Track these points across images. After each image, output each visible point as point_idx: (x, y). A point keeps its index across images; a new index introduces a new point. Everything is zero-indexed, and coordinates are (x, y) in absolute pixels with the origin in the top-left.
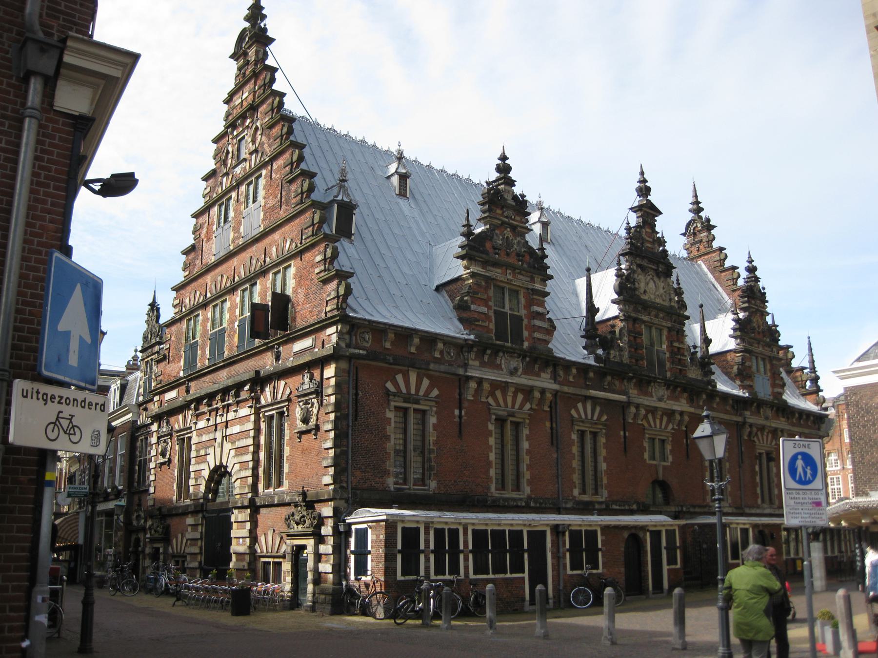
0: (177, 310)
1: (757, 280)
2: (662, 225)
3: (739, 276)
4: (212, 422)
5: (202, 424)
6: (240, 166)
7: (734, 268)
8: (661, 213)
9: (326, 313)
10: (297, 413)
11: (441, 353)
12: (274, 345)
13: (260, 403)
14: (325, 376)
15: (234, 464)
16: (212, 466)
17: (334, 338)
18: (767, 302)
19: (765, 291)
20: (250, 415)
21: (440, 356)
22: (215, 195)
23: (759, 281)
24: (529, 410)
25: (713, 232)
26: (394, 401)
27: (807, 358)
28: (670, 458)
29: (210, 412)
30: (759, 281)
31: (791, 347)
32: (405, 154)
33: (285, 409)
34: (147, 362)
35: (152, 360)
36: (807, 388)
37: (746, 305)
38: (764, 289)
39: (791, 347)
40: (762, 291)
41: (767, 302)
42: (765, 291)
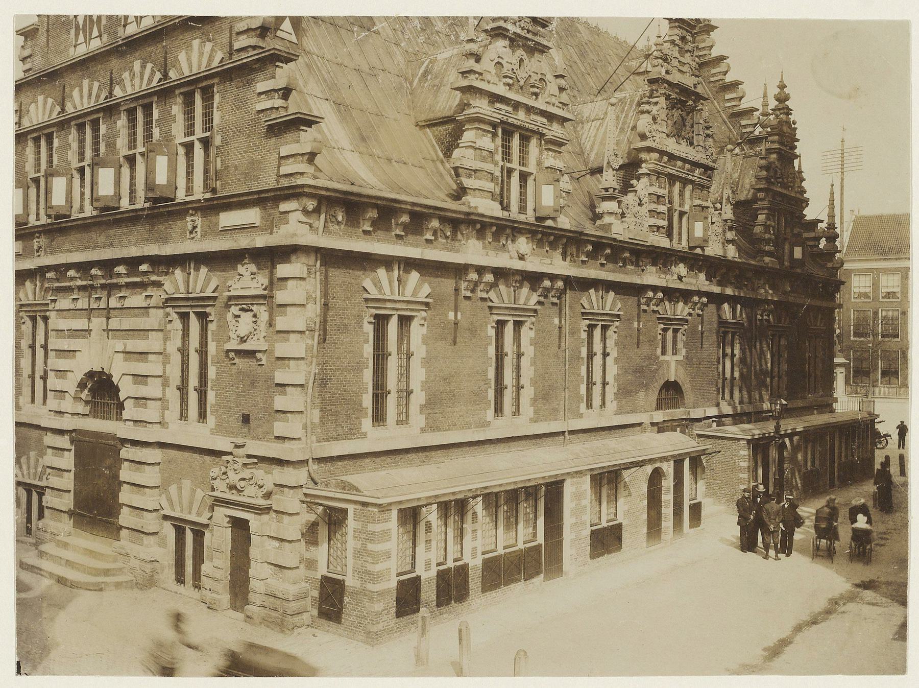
1: (788, 111)
5: (64, 303)
11: (435, 233)
12: (188, 209)
18: (798, 140)
19: (796, 126)
21: (433, 238)
23: (791, 114)
26: (374, 308)
27: (827, 211)
28: (684, 352)
30: (791, 114)
36: (821, 246)
37: (776, 146)
38: (794, 123)
40: (793, 126)
41: (798, 140)
42: (796, 126)
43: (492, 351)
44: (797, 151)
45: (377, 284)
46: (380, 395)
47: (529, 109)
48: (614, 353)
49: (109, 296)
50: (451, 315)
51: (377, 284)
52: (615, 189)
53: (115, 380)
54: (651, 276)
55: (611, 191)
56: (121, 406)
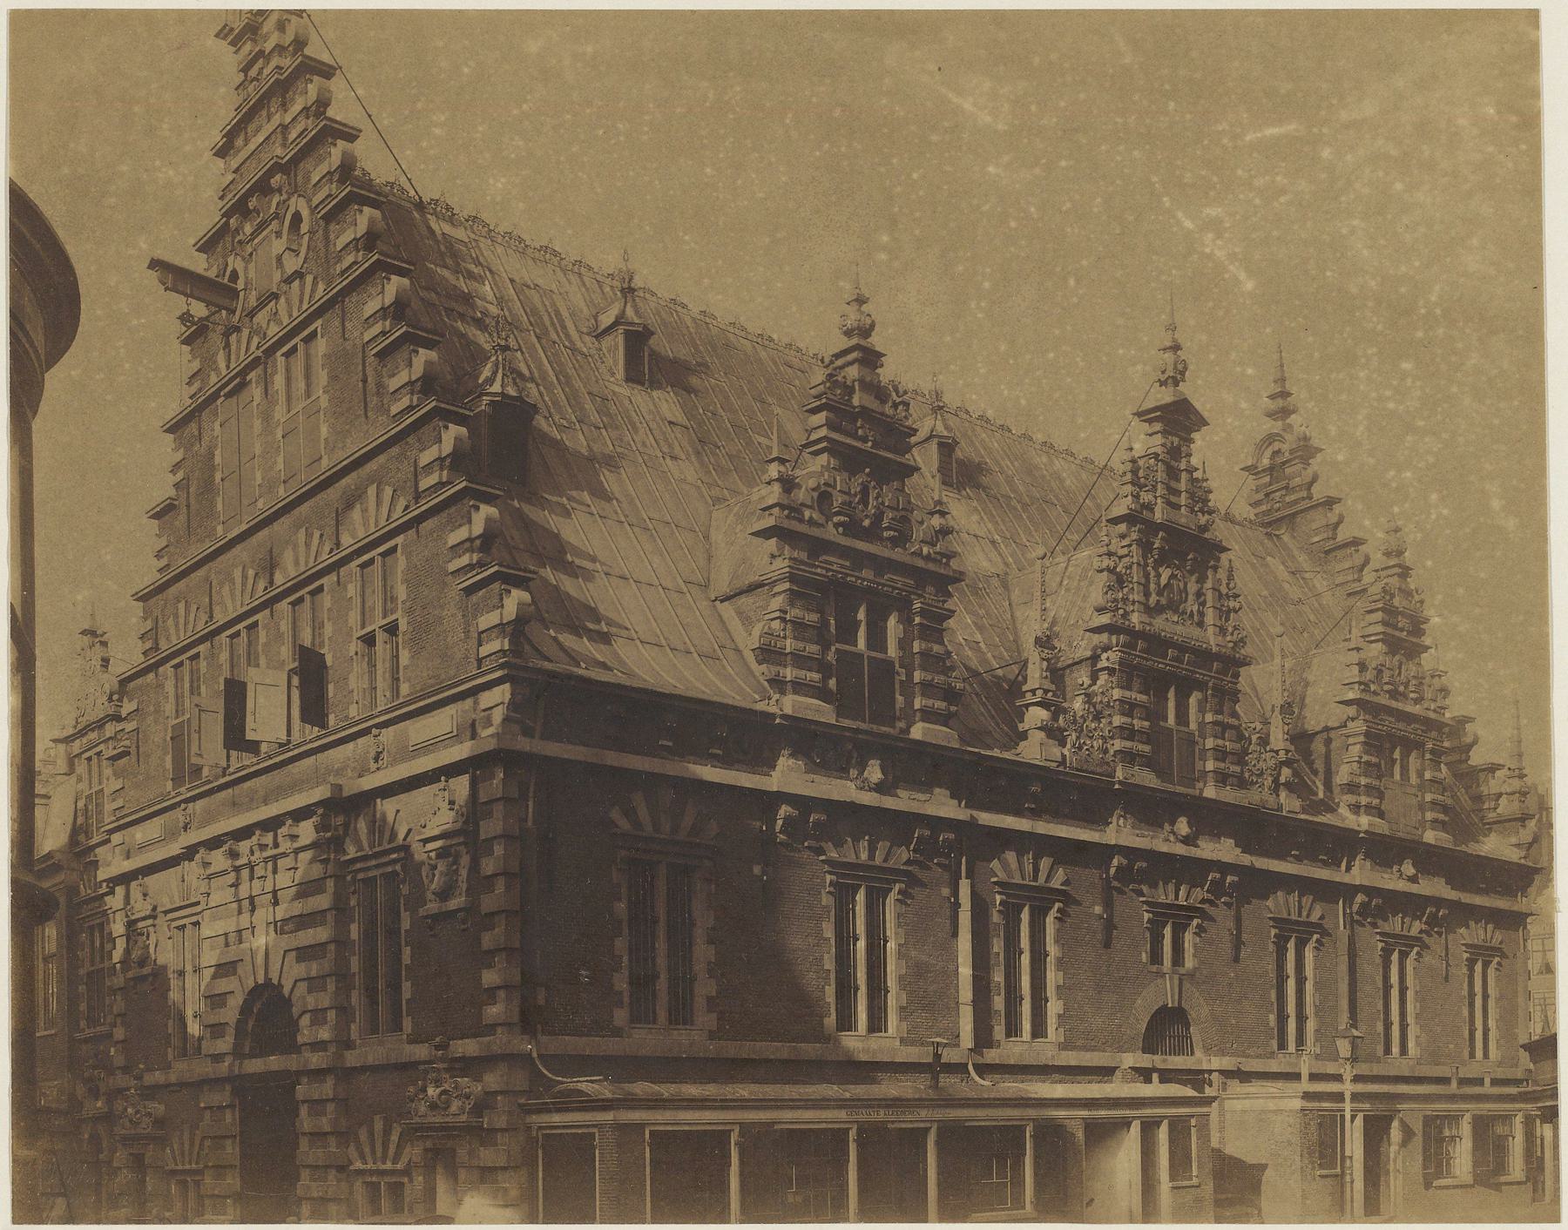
0: (149, 645)
1: (1405, 572)
2: (1203, 449)
3: (1367, 561)
4: (244, 891)
6: (268, 308)
7: (1356, 542)
8: (1206, 424)
9: (480, 661)
10: (424, 874)
13: (345, 852)
14: (483, 798)
15: (296, 981)
16: (251, 984)
17: (498, 715)
20: (326, 878)
22: (214, 379)
24: (905, 864)
25: (1315, 463)
29: (237, 869)
31: (1470, 720)
32: (638, 282)
33: (398, 867)
34: (89, 759)
35: (99, 754)
39: (1470, 720)
42: (1422, 596)
43: (829, 931)
44: (1427, 641)
45: (629, 813)
46: (642, 983)
47: (882, 565)
48: (1052, 949)
49: (275, 871)
50: (757, 870)
51: (629, 813)
52: (1046, 691)
53: (295, 1011)
54: (1119, 832)
55: (1039, 693)
56: (294, 1025)
